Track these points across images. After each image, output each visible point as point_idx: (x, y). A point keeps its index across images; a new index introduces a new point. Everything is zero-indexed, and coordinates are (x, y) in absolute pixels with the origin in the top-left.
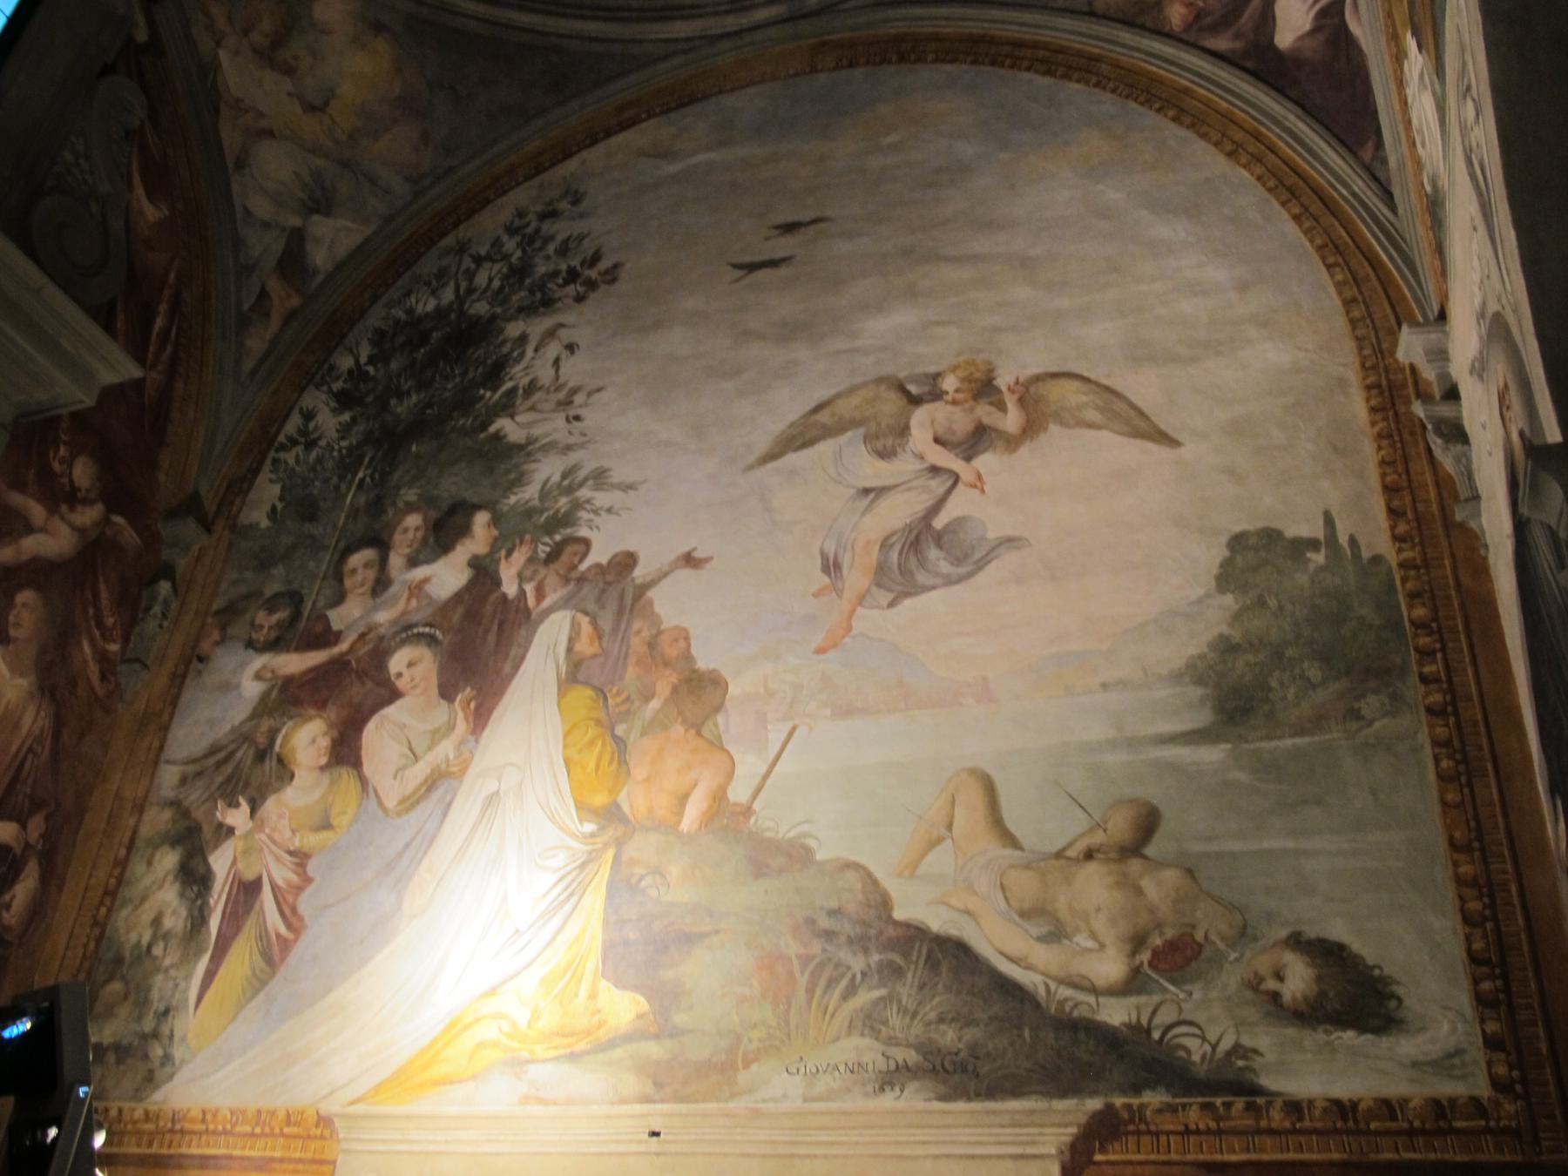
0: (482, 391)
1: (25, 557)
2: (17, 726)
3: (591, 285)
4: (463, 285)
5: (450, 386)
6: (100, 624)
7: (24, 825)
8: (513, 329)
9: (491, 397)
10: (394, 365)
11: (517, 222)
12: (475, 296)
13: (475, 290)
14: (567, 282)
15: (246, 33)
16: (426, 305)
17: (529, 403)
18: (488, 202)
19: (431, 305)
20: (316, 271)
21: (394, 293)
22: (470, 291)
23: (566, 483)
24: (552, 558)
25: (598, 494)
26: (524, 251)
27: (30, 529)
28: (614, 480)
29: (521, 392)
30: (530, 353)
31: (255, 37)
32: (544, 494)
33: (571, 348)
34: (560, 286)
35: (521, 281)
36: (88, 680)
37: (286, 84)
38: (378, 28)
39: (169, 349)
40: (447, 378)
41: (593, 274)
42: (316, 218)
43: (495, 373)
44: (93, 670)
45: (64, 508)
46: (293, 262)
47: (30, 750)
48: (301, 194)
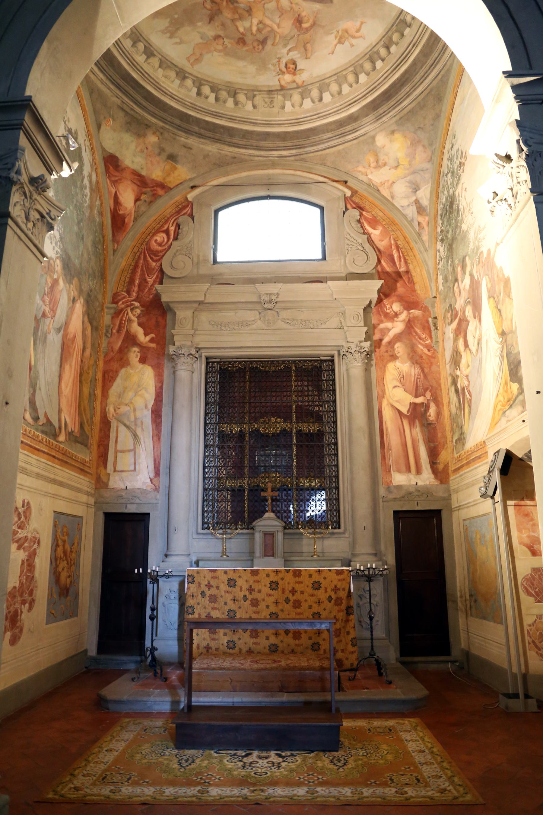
1: (392, 337)
2: (411, 375)
3: (464, 164)
6: (421, 339)
7: (425, 396)
9: (459, 219)
10: (445, 223)
15: (370, 166)
16: (444, 200)
20: (427, 206)
24: (479, 261)
27: (389, 330)
31: (373, 165)
32: (474, 243)
33: (465, 190)
36: (425, 354)
37: (387, 168)
38: (393, 132)
39: (402, 260)
42: (418, 192)
44: (425, 351)
45: (396, 319)
46: (421, 210)
47: (417, 378)
48: (411, 190)
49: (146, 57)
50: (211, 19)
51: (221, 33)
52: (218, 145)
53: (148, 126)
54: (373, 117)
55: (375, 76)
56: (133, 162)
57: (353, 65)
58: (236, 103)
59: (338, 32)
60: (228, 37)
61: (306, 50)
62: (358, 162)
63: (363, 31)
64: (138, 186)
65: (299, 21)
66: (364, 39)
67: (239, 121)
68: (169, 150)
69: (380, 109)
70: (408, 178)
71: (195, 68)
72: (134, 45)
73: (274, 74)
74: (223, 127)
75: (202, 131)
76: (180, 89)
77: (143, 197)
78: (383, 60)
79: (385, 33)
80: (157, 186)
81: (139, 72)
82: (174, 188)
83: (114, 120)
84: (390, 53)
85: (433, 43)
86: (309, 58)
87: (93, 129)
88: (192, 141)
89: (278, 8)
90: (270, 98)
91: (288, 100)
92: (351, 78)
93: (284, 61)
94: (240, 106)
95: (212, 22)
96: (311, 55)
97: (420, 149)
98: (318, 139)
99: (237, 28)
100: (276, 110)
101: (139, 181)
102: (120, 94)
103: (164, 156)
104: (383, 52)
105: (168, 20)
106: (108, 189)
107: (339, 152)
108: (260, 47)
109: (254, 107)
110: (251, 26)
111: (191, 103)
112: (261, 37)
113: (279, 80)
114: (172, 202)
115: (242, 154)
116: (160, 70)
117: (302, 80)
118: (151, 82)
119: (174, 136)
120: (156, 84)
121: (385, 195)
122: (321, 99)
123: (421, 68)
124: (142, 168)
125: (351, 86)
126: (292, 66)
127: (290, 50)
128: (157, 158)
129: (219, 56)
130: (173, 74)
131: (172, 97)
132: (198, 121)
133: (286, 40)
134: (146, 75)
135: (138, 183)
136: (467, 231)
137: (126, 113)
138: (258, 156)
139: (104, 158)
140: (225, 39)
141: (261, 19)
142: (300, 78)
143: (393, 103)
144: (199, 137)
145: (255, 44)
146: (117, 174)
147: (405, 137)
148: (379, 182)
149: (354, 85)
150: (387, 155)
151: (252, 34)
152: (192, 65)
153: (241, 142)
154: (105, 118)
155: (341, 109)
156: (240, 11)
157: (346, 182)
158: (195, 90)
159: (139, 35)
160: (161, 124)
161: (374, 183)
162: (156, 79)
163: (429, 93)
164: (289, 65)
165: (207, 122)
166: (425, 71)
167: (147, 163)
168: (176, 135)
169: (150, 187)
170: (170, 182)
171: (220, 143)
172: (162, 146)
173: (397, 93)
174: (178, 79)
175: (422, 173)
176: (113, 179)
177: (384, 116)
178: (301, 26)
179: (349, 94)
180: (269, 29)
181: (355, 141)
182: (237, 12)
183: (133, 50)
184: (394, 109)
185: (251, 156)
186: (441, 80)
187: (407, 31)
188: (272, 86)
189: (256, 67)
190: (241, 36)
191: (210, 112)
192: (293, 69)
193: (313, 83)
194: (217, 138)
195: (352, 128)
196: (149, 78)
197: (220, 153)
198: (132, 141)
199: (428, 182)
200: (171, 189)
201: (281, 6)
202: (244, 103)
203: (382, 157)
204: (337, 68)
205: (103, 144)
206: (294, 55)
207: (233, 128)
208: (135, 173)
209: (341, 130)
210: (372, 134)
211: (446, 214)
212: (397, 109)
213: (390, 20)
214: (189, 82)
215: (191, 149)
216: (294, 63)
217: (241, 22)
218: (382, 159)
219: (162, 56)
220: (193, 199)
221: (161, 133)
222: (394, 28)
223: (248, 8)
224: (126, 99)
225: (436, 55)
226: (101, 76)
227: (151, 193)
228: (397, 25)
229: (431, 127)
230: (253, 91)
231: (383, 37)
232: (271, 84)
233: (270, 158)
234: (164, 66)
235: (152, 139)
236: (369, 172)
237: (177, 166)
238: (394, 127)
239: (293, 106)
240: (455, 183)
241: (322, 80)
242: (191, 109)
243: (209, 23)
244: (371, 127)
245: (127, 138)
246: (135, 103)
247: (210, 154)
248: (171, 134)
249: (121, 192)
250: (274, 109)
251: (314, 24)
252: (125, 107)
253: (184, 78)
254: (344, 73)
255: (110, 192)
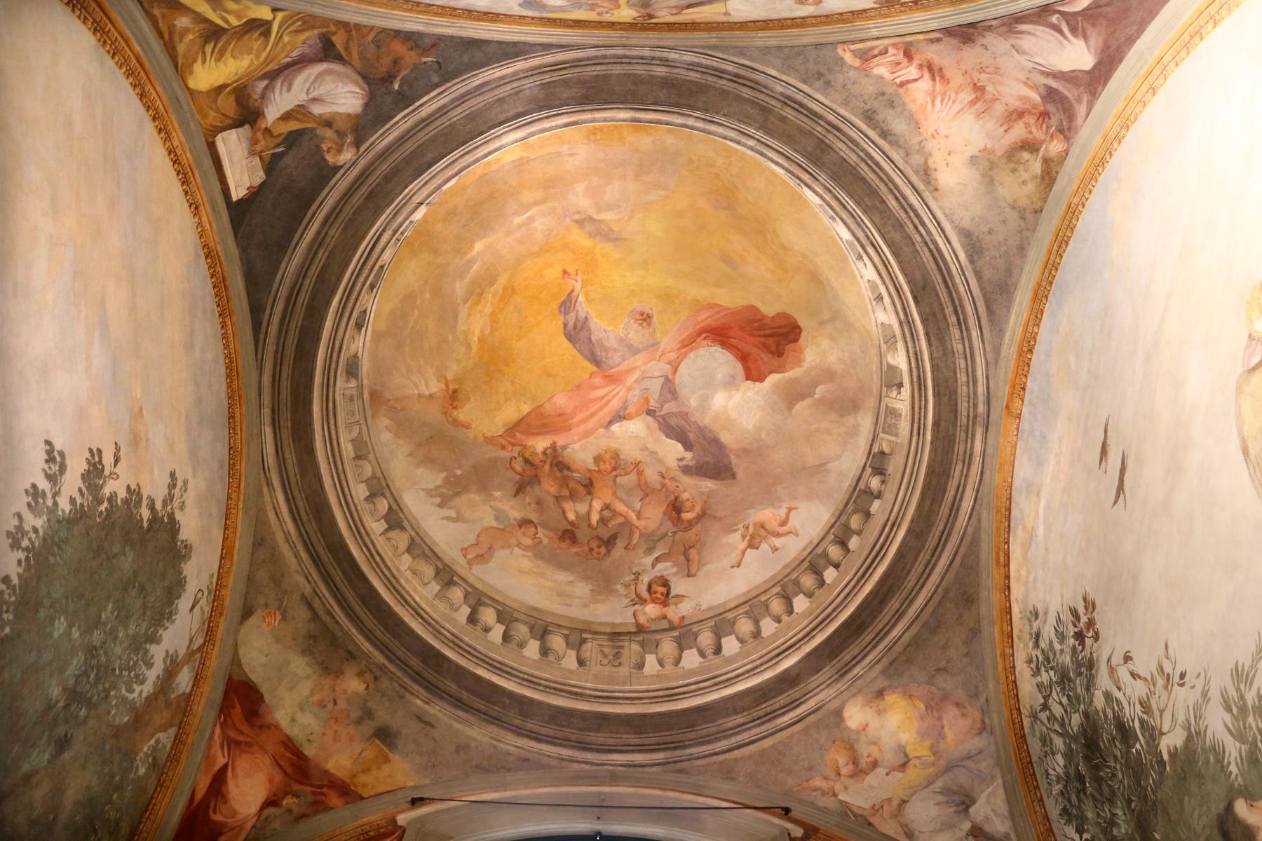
0: (1134, 750)
3: (1091, 623)
4: (1057, 727)
5: (1120, 776)
8: (1099, 701)
11: (1033, 666)
12: (1067, 721)
13: (1063, 719)
14: (1082, 643)
16: (1058, 763)
17: (1157, 714)
18: (1015, 682)
19: (1060, 760)
21: (1043, 785)
22: (1062, 724)
23: (1235, 710)
25: (1255, 687)
26: (1052, 668)
28: (1248, 663)
29: (1145, 717)
30: (1119, 695)
31: (844, 771)
33: (1127, 658)
34: (1082, 651)
35: (1070, 680)
37: (881, 771)
38: (880, 694)
40: (1114, 775)
41: (1084, 619)
42: (971, 810)
43: (1124, 732)
49: (386, 526)
50: (520, 490)
51: (533, 516)
52: (494, 730)
53: (351, 656)
54: (833, 671)
55: (824, 597)
56: (293, 720)
57: (779, 582)
58: (545, 651)
59: (747, 528)
60: (545, 526)
61: (688, 560)
62: (811, 768)
63: (794, 521)
64: (286, 774)
65: (676, 508)
66: (797, 535)
67: (546, 687)
68: (383, 716)
69: (845, 653)
70: (939, 783)
71: (474, 571)
72: (371, 498)
73: (626, 601)
74: (511, 695)
75: (465, 695)
76: (436, 602)
77: (288, 801)
78: (837, 566)
79: (833, 521)
80: (329, 787)
81: (365, 549)
82: (370, 797)
83: (284, 618)
84: (848, 551)
85: (930, 510)
86: (694, 576)
87: (232, 600)
88: (437, 711)
89: (639, 485)
90: (613, 647)
91: (651, 653)
92: (777, 606)
93: (645, 579)
94: (552, 658)
95: (521, 494)
96: (698, 569)
97: (951, 713)
98: (714, 729)
99: (564, 513)
100: (624, 671)
101: (292, 765)
102: (315, 575)
103: (367, 728)
104: (834, 552)
105: (444, 475)
106: (209, 747)
107: (763, 752)
108: (603, 550)
109: (581, 662)
110: (589, 513)
111: (453, 634)
112: (605, 533)
113: (635, 615)
114: (360, 822)
115: (544, 755)
116: (406, 557)
117: (681, 615)
118: (385, 576)
119: (402, 691)
120: (392, 579)
121: (891, 833)
122: (718, 650)
123: (916, 559)
124: (309, 740)
125: (778, 620)
126: (661, 589)
127: (657, 560)
128: (352, 729)
129: (524, 556)
130: (429, 571)
131: (417, 612)
132: (460, 674)
133: (651, 540)
134: (378, 559)
135: (289, 770)
136: (1189, 739)
137: (315, 616)
138: (579, 762)
139: (230, 678)
140: (540, 529)
141: (608, 501)
142: (676, 612)
143: (869, 638)
144: (455, 706)
145: (594, 544)
146: (245, 728)
147: (910, 697)
148: (865, 806)
149: (785, 618)
150: (875, 744)
151: (590, 526)
152: (469, 563)
153: (544, 731)
154: (266, 605)
155: (761, 665)
156: (572, 484)
157: (787, 811)
158: (466, 611)
159: (384, 485)
160: (381, 659)
161: (854, 809)
162: (395, 572)
163: (943, 597)
164: (655, 587)
165: (479, 679)
166: (924, 562)
167: (324, 734)
168: (405, 688)
169: (312, 786)
170: (364, 785)
171: (498, 725)
172: (369, 704)
173: (875, 617)
174: (438, 584)
175: (969, 763)
176: (232, 733)
177: (854, 666)
178: (679, 517)
179: (775, 636)
180: (621, 520)
181: (798, 727)
182: (567, 486)
183: (368, 506)
184: (874, 647)
185: (562, 759)
186: (962, 565)
187: (876, 506)
188: (621, 624)
189: (591, 587)
190: (569, 527)
191: (487, 660)
192: (662, 594)
193: (702, 621)
194: (494, 714)
195: (788, 700)
196: (382, 566)
197: (495, 747)
198: (308, 677)
199: (993, 778)
200: (362, 798)
201: (646, 482)
202: (561, 654)
203: (864, 750)
204: (749, 591)
205: (241, 652)
206: (665, 568)
207: (531, 701)
208: (291, 748)
209: (766, 707)
210: (834, 705)
211: (1082, 791)
212: (881, 646)
213: (840, 497)
214: (457, 594)
215: (433, 726)
216: (665, 583)
217: (571, 503)
218: (865, 755)
219: (417, 533)
220: (409, 823)
221: (376, 679)
222: (851, 507)
223: (587, 482)
224: (323, 589)
225: (941, 527)
226: (290, 526)
227: (310, 799)
228: (854, 502)
229: (965, 660)
230: (582, 631)
231: (832, 526)
232: (618, 620)
233: (606, 767)
234: (417, 552)
235: (353, 685)
236: (838, 786)
237: (391, 755)
238: (881, 683)
239: (661, 663)
240: (1080, 690)
241: (720, 614)
242: (451, 645)
243: (515, 496)
244: (831, 692)
245: (300, 665)
246: (339, 603)
247: (473, 744)
248: (396, 685)
249: (239, 771)
250: (620, 669)
251: (703, 515)
252: (317, 604)
253: (449, 583)
254: (763, 598)
255: (208, 758)
